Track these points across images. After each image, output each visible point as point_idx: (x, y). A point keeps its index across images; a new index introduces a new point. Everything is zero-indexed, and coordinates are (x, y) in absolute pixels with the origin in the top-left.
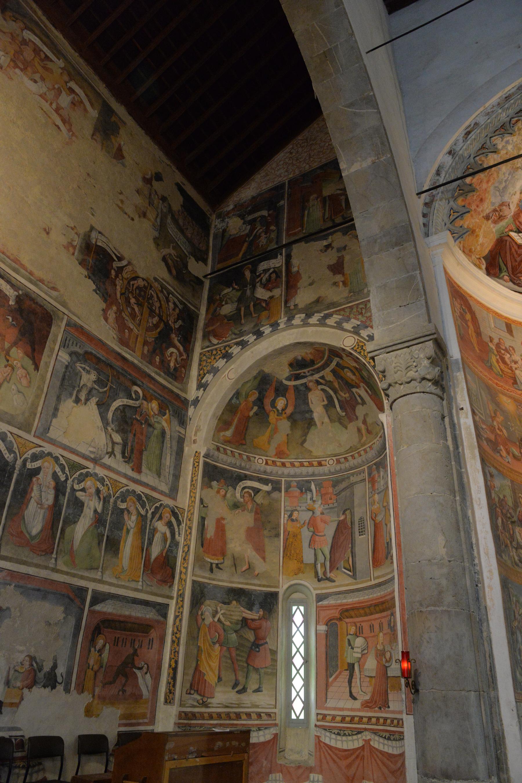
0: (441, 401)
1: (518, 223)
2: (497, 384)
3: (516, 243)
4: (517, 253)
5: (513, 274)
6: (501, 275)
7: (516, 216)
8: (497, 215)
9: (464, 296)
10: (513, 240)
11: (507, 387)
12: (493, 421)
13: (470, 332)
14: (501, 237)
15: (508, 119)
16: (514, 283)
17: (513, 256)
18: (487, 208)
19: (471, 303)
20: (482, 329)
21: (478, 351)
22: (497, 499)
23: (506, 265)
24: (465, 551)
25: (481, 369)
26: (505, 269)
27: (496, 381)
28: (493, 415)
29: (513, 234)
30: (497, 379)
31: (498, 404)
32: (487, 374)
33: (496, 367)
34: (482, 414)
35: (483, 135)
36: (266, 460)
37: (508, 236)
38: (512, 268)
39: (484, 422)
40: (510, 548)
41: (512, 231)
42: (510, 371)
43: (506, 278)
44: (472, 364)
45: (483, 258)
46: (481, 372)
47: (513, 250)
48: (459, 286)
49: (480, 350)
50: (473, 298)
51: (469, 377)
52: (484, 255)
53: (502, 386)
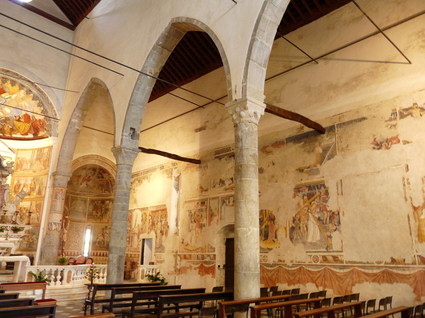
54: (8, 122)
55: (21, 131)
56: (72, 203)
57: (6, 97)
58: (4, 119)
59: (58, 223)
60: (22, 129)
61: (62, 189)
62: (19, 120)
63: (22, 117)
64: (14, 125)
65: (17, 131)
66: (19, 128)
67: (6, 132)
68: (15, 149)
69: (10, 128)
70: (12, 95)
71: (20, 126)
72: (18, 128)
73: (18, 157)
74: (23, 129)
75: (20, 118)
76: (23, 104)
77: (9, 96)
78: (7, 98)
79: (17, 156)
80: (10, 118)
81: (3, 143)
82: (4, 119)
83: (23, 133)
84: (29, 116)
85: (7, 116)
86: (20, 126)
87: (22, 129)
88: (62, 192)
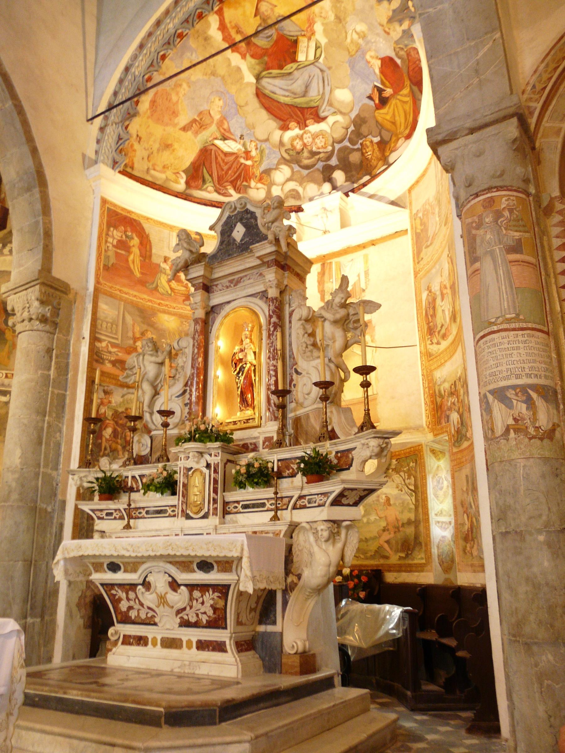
0: (51, 336)
1: (223, 131)
2: (159, 304)
3: (222, 151)
4: (223, 161)
5: (219, 184)
6: (205, 187)
7: (220, 124)
8: (198, 124)
9: (135, 220)
10: (219, 149)
11: (175, 305)
12: (135, 342)
13: (131, 258)
14: (205, 147)
15: (174, 31)
16: (219, 193)
17: (220, 165)
18: (183, 119)
19: (146, 226)
20: (154, 251)
21: (138, 274)
22: (109, 414)
23: (211, 176)
24: (42, 460)
25: (135, 293)
26: (210, 179)
27: (159, 301)
28: (138, 335)
29: (217, 142)
30: (163, 299)
31: (152, 325)
32: (145, 296)
33: (163, 288)
34: (117, 339)
35: (153, 50)
36: (6, 374)
37: (213, 144)
38: (218, 178)
39: (114, 345)
40: (121, 453)
41: (216, 139)
42: (184, 289)
43: (211, 189)
44: (120, 291)
45: (184, 171)
46: (135, 296)
47: (219, 159)
48: (129, 212)
49: (142, 273)
50: (151, 219)
51: (103, 306)
52: (184, 167)
53: (167, 305)
54: (364, 130)
55: (402, 127)
56: (231, 133)
57: (311, 57)
58: (352, 128)
59: (523, 389)
60: (400, 119)
61: (492, 200)
62: (383, 102)
63: (383, 83)
64: (380, 127)
65: (394, 139)
66: (394, 123)
67: (374, 162)
68: (405, 193)
69: (378, 143)
70: (313, 33)
71: (394, 115)
72: (392, 128)
73: (414, 212)
74: (403, 121)
75: (380, 91)
76: (355, 36)
77: (313, 45)
78: (317, 59)
79: (411, 213)
80: (365, 115)
81: (371, 197)
82: (352, 128)
83: (407, 132)
84: (391, 59)
85: (353, 115)
86: (394, 115)
87: (400, 119)
88: (498, 214)
